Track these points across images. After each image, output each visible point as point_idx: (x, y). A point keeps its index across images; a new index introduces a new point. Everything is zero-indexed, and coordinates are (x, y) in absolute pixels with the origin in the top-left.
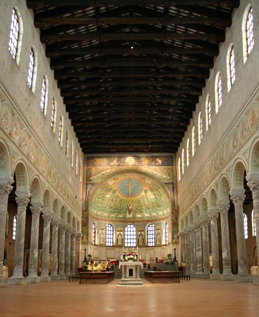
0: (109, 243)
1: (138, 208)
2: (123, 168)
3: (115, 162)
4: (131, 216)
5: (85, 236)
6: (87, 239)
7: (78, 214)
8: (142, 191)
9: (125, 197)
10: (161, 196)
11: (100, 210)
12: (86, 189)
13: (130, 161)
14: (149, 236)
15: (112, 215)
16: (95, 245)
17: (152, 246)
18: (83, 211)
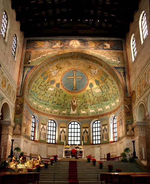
0: (51, 140)
1: (82, 104)
2: (68, 51)
3: (58, 45)
4: (75, 112)
5: (18, 126)
6: (20, 129)
7: (10, 99)
8: (87, 85)
9: (69, 92)
10: (108, 88)
11: (42, 104)
12: (24, 72)
13: (75, 44)
14: (94, 133)
15: (55, 111)
16: (34, 140)
17: (98, 144)
18: (17, 96)
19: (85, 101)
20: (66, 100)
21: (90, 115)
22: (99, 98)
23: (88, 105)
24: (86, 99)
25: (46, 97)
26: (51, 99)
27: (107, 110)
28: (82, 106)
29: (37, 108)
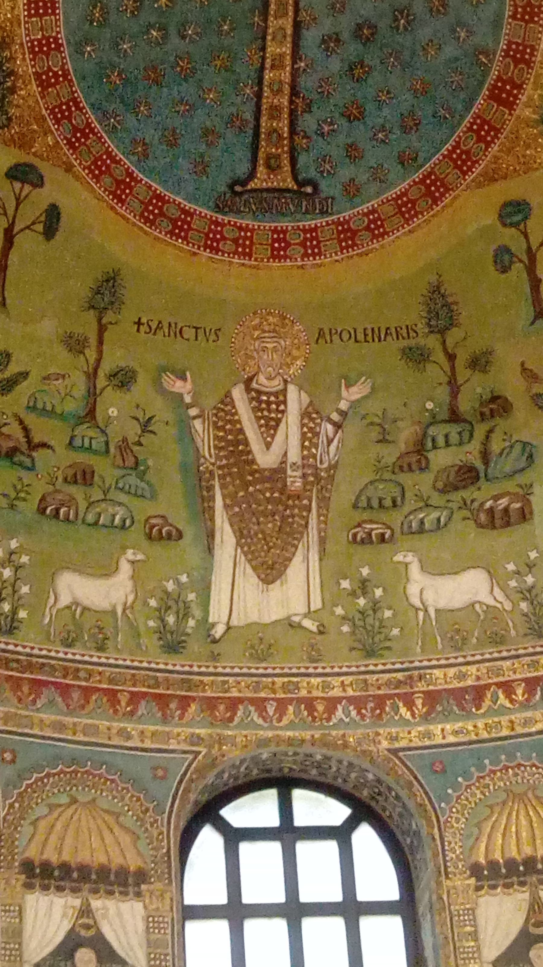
23: (531, 456)
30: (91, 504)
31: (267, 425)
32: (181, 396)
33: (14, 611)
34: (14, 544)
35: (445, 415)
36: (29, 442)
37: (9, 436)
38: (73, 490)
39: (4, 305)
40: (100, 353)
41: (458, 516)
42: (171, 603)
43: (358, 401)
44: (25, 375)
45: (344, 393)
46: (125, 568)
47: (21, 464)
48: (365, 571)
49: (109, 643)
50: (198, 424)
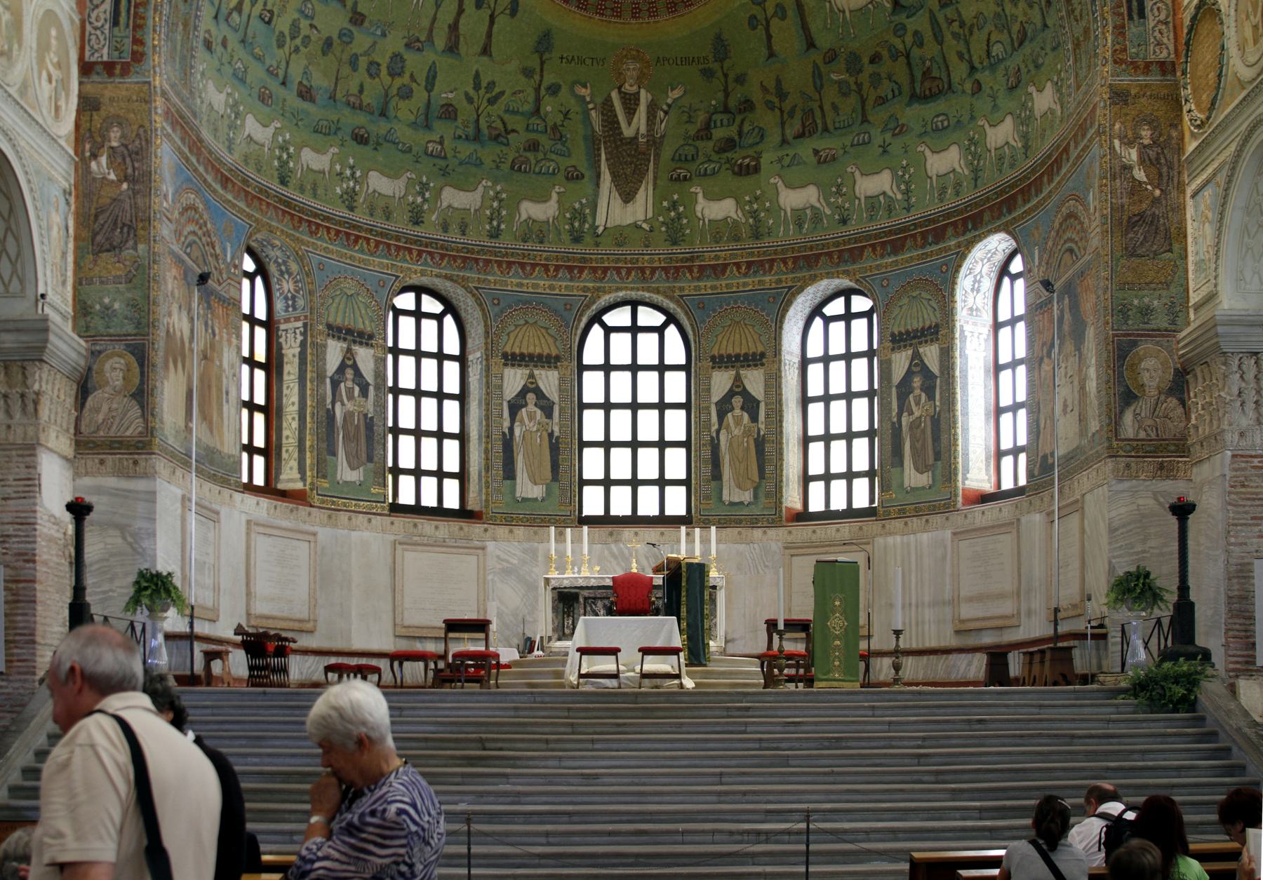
1: (705, 132)
4: (640, 210)
5: (115, 370)
11: (324, 132)
15: (453, 198)
19: (732, 103)
20: (554, 90)
21: (784, 236)
22: (869, 69)
23: (762, 136)
24: (741, 79)
25: (363, 62)
26: (406, 79)
27: (943, 190)
28: (707, 146)
29: (283, 182)
30: (538, 162)
31: (629, 113)
32: (584, 97)
33: (499, 226)
34: (499, 188)
35: (721, 109)
36: (506, 130)
37: (496, 129)
38: (528, 154)
39: (491, 56)
40: (542, 76)
41: (724, 167)
42: (577, 215)
43: (677, 99)
44: (502, 93)
45: (670, 94)
46: (554, 196)
47: (502, 143)
48: (676, 197)
49: (546, 239)
50: (593, 113)
